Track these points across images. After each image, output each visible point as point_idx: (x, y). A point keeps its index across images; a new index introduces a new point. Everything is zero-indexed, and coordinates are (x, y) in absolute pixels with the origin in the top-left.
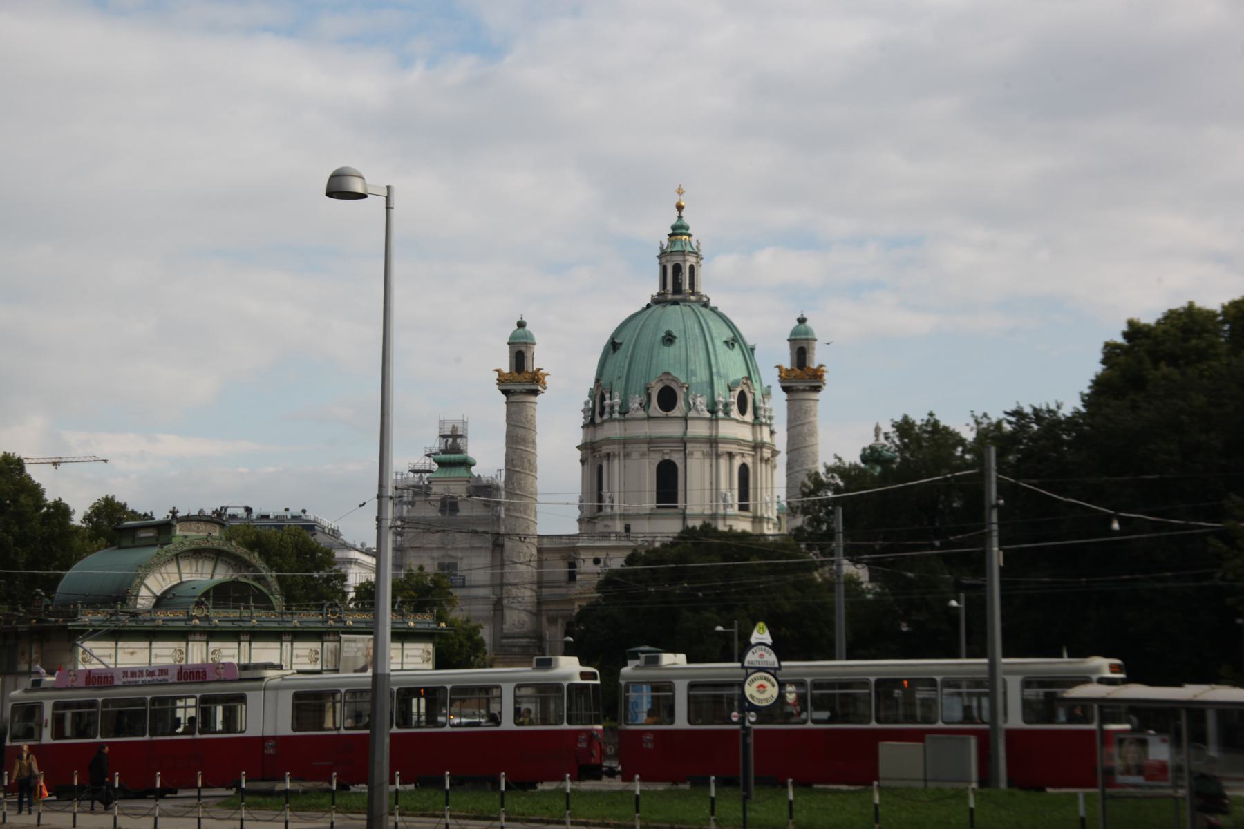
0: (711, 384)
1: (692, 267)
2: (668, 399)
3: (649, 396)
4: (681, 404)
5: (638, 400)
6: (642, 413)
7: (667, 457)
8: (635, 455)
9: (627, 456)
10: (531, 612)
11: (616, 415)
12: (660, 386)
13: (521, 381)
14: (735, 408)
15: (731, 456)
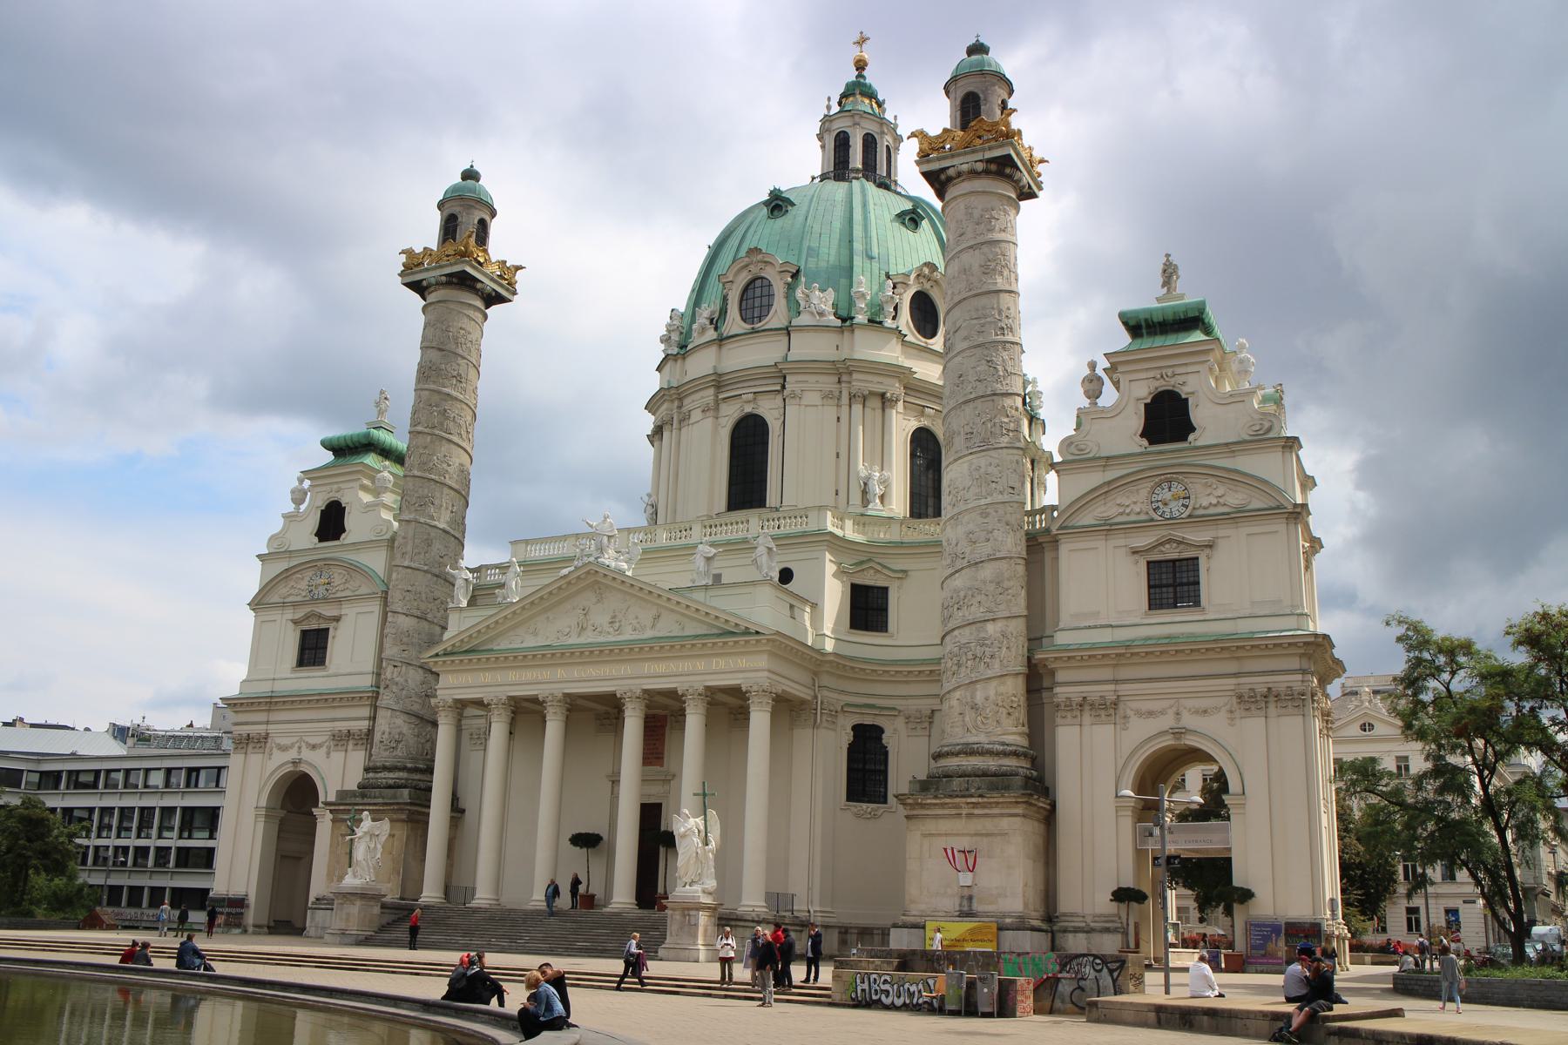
0: (851, 268)
1: (870, 143)
2: (755, 298)
3: (725, 299)
4: (779, 304)
5: (706, 314)
6: (711, 334)
7: (748, 409)
8: (696, 415)
9: (685, 419)
10: (417, 716)
11: (675, 350)
12: (744, 278)
13: (458, 272)
14: (905, 320)
15: (885, 401)
